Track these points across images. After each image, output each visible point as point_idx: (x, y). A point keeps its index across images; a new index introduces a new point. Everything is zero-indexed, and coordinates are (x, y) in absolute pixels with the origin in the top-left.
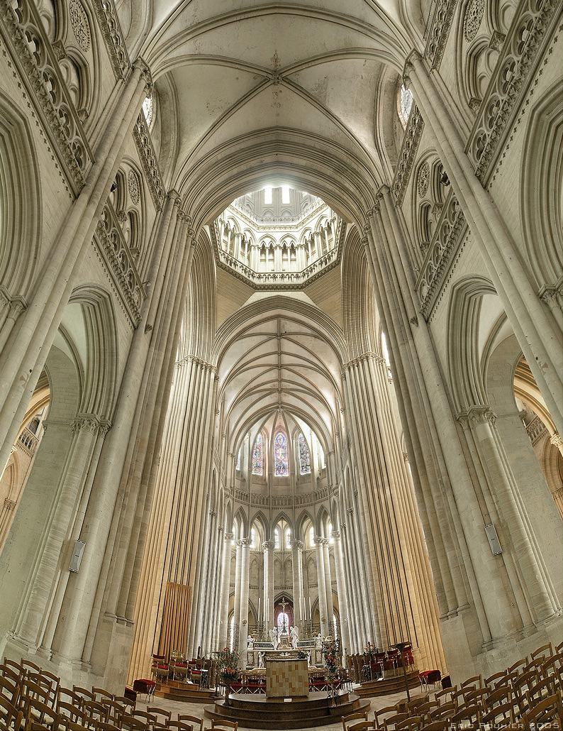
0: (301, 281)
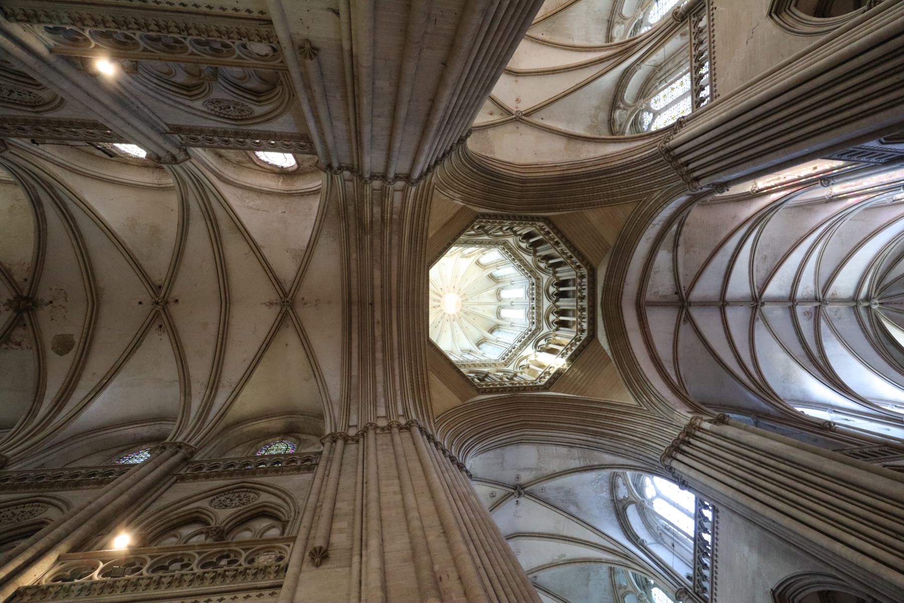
0: (584, 271)
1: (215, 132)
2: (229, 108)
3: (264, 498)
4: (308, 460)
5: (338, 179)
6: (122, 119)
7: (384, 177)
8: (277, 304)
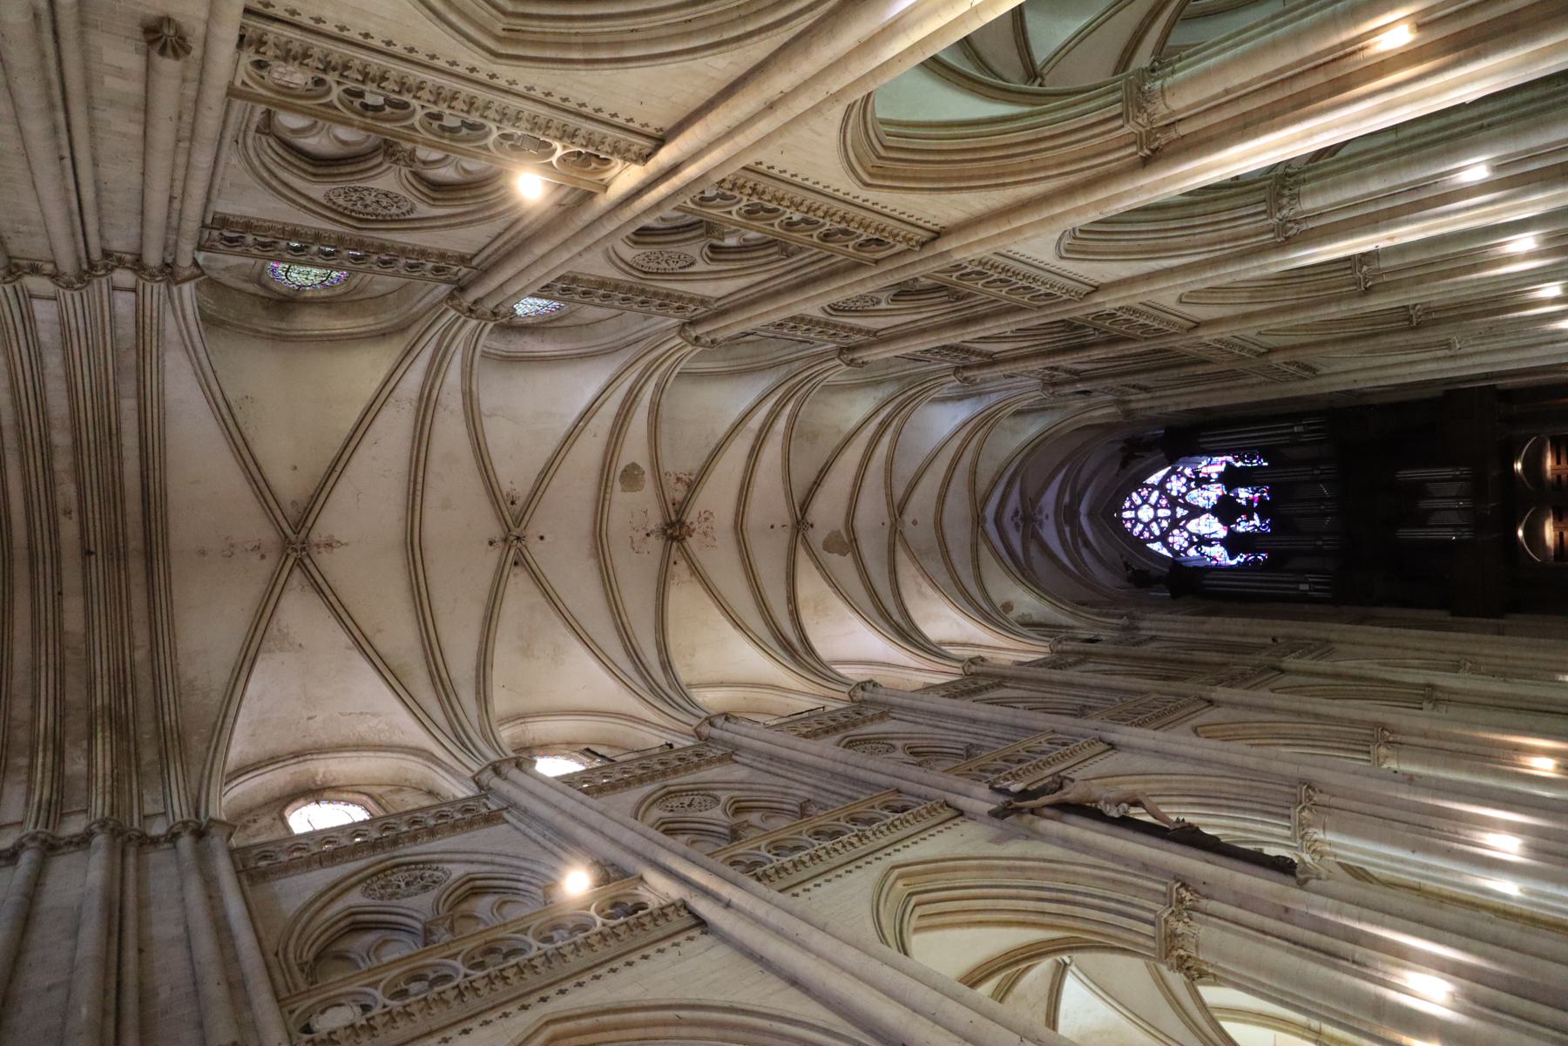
1: (432, 833)
2: (407, 884)
3: (318, 191)
4: (230, 240)
5: (180, 810)
6: (563, 812)
7: (51, 848)
8: (318, 546)
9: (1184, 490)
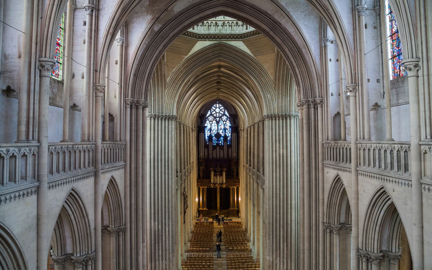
9: (223, 120)
